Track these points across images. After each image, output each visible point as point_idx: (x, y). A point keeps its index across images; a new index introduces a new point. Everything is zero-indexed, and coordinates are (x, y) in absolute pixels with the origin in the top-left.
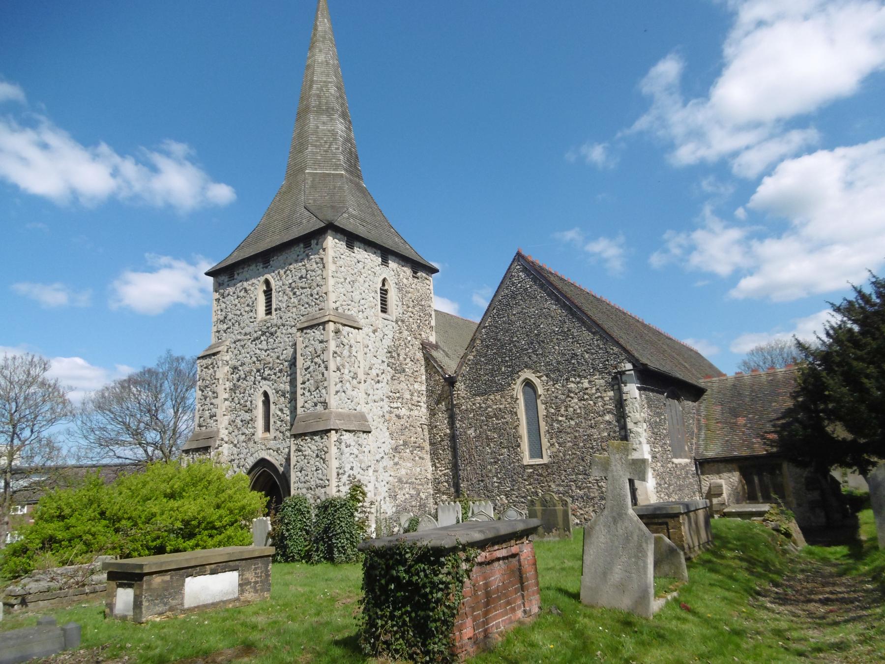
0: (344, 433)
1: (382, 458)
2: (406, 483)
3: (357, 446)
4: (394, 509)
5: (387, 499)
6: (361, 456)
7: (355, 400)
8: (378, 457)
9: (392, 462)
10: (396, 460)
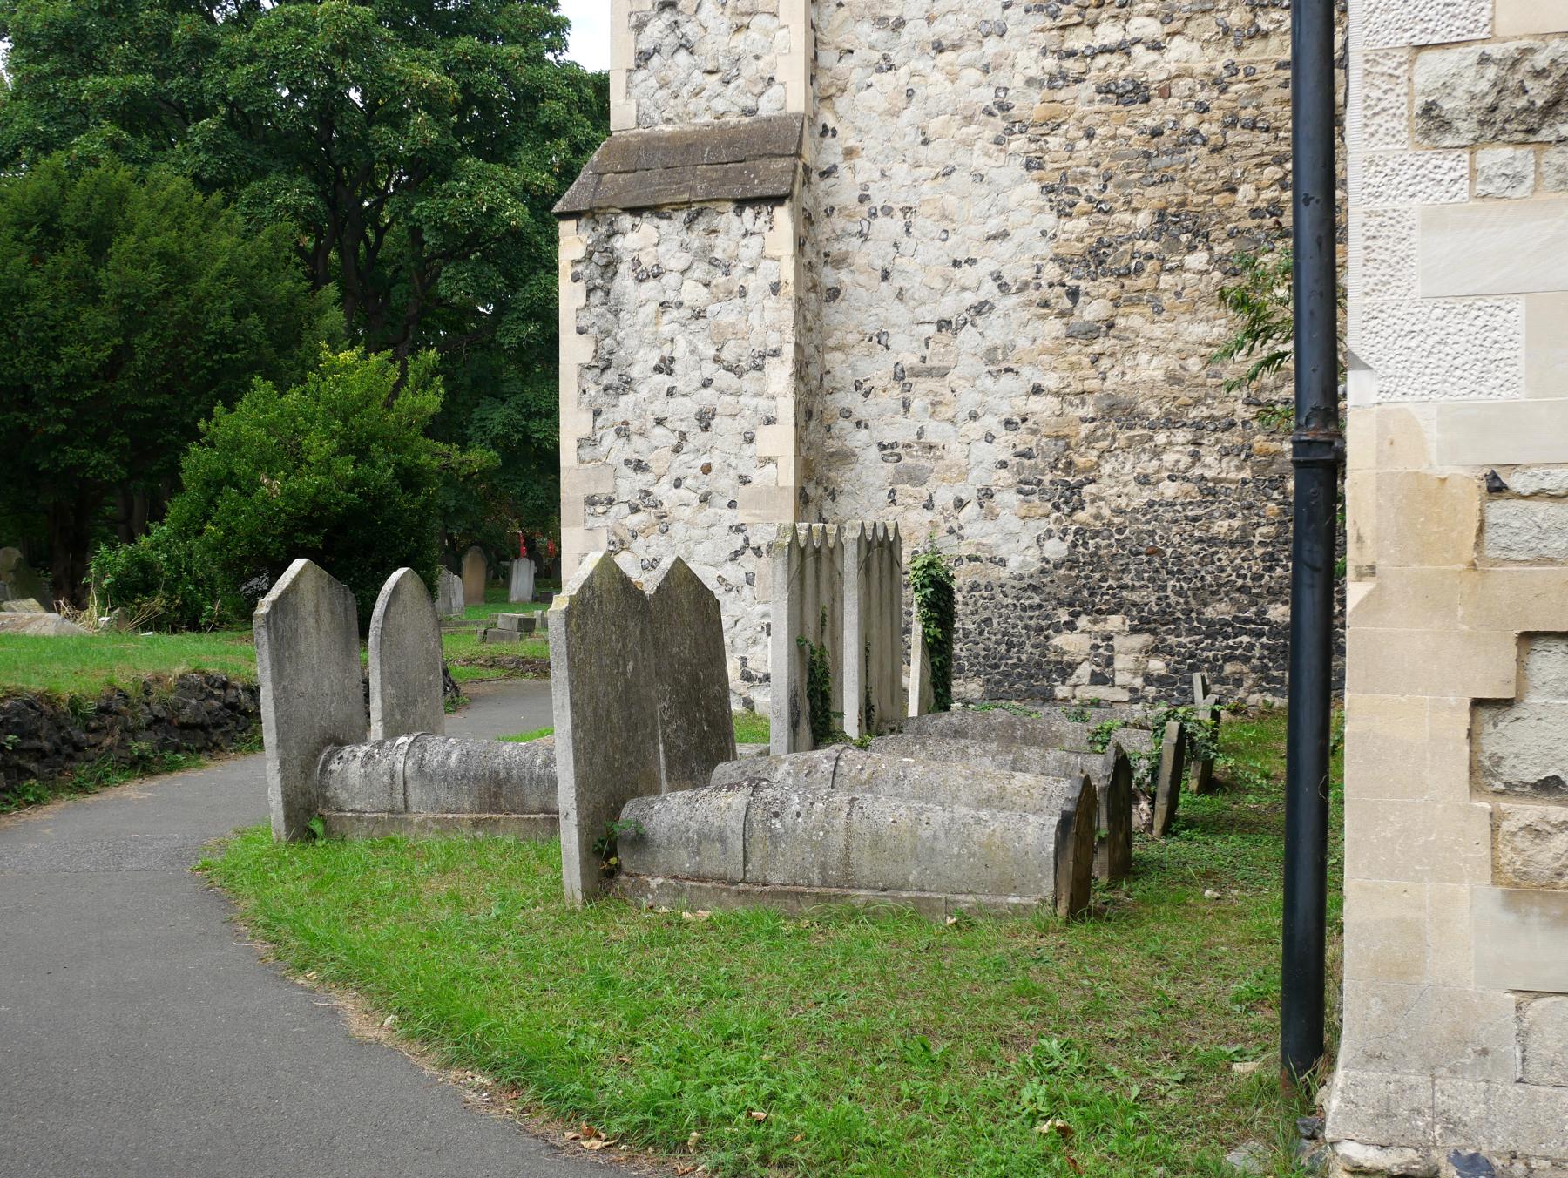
0: (626, 221)
1: (980, 309)
2: (1170, 422)
3: (701, 270)
4: (1056, 549)
5: (1008, 499)
6: (727, 314)
7: (750, 69)
8: (950, 307)
9: (1055, 326)
10: (1092, 311)
